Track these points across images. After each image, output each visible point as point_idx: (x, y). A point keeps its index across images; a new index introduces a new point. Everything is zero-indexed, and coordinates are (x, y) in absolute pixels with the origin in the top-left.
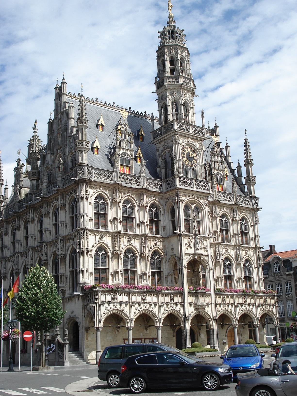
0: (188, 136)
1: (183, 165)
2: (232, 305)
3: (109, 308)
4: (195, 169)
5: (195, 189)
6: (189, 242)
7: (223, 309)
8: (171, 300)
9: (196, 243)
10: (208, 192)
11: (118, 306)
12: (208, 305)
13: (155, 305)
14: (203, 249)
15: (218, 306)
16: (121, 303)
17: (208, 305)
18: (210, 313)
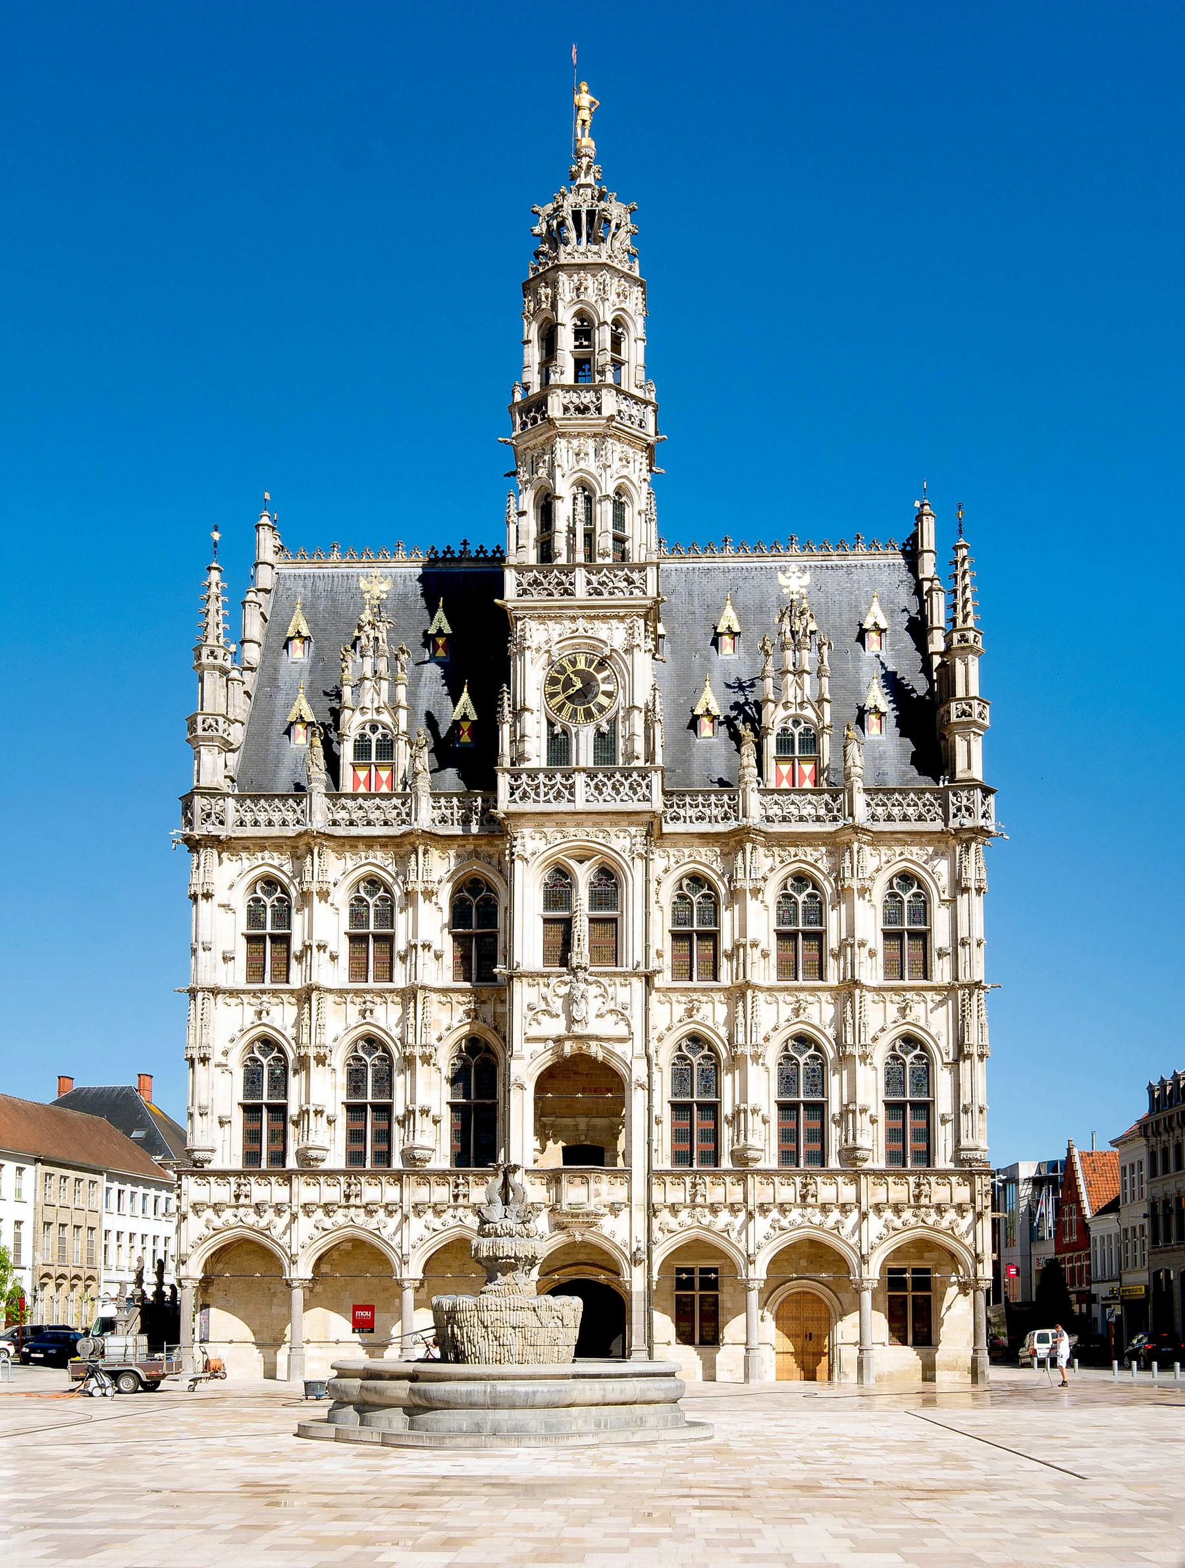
0: (571, 613)
1: (551, 724)
2: (733, 1209)
3: (218, 1223)
4: (605, 728)
5: (580, 805)
6: (545, 999)
7: (689, 1221)
8: (456, 1197)
9: (569, 1000)
10: (645, 806)
11: (252, 1219)
12: (614, 1209)
13: (390, 1213)
14: (614, 1018)
15: (665, 1216)
16: (258, 1208)
17: (614, 1209)
18: (621, 1237)
